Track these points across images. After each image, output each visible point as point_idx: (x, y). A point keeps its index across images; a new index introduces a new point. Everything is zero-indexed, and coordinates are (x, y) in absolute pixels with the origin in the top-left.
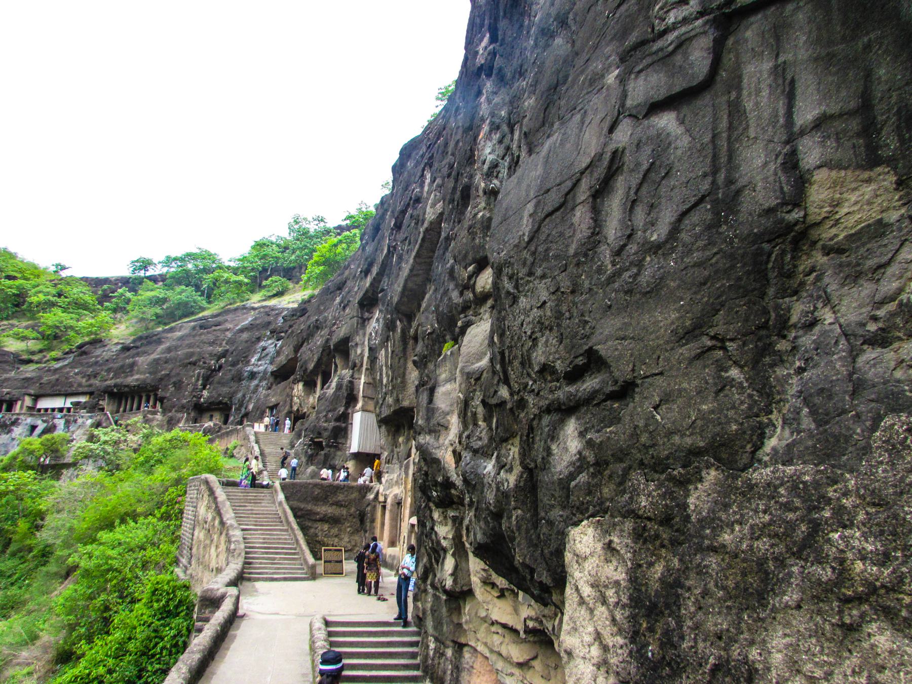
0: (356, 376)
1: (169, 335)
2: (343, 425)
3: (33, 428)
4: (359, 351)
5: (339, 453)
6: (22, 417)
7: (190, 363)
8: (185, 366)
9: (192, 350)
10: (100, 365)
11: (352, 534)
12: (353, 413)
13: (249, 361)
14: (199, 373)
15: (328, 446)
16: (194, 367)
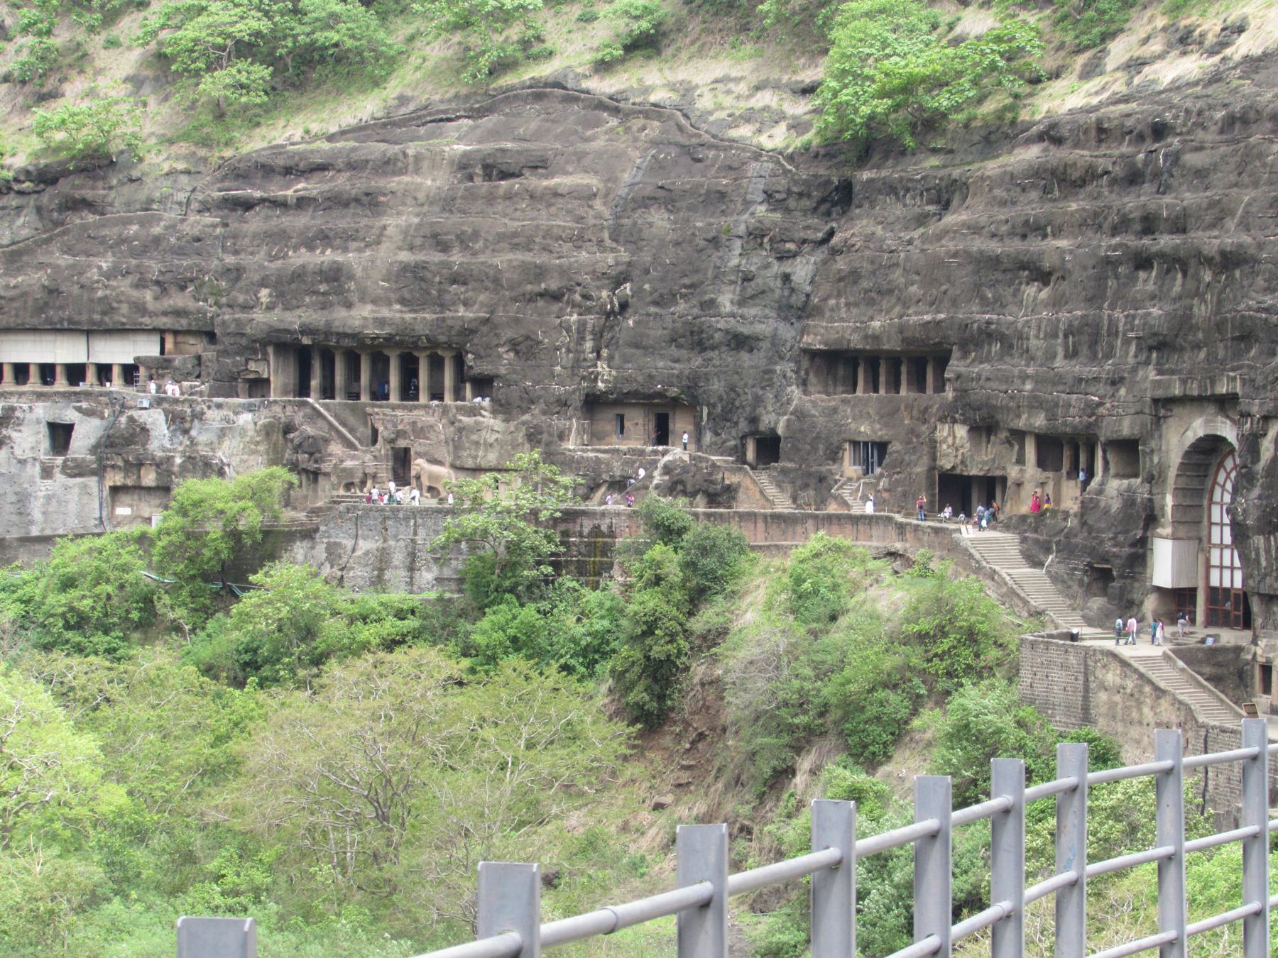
0: (1155, 491)
1: (394, 183)
2: (1141, 551)
3: (60, 434)
4: (1156, 460)
5: (1136, 585)
6: (13, 401)
7: (541, 295)
8: (532, 298)
9: (527, 257)
10: (180, 252)
11: (1234, 689)
12: (1153, 536)
13: (712, 303)
14: (582, 325)
15: (1122, 576)
16: (555, 307)
